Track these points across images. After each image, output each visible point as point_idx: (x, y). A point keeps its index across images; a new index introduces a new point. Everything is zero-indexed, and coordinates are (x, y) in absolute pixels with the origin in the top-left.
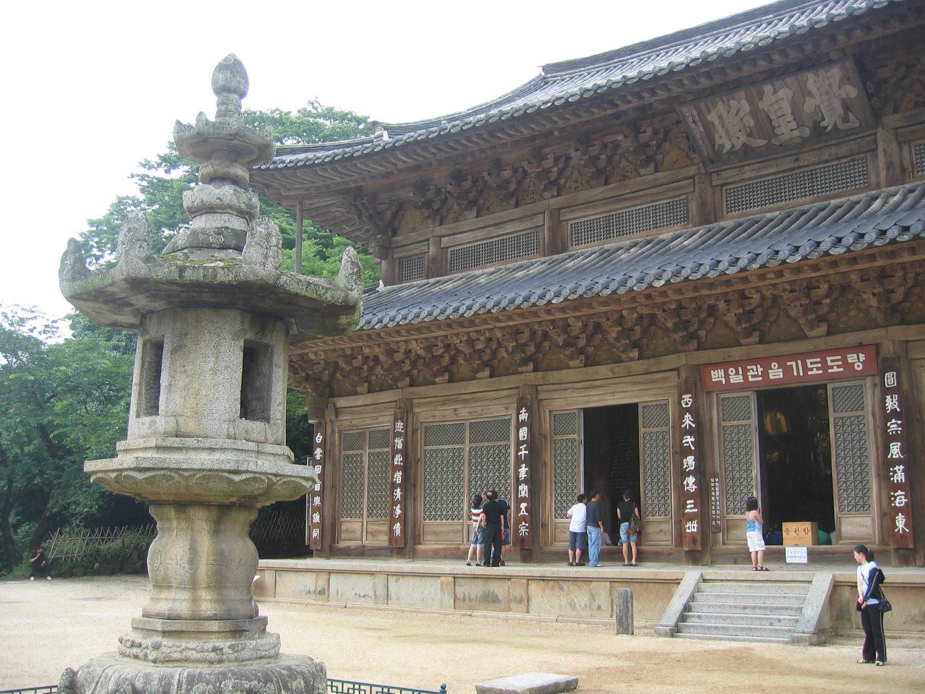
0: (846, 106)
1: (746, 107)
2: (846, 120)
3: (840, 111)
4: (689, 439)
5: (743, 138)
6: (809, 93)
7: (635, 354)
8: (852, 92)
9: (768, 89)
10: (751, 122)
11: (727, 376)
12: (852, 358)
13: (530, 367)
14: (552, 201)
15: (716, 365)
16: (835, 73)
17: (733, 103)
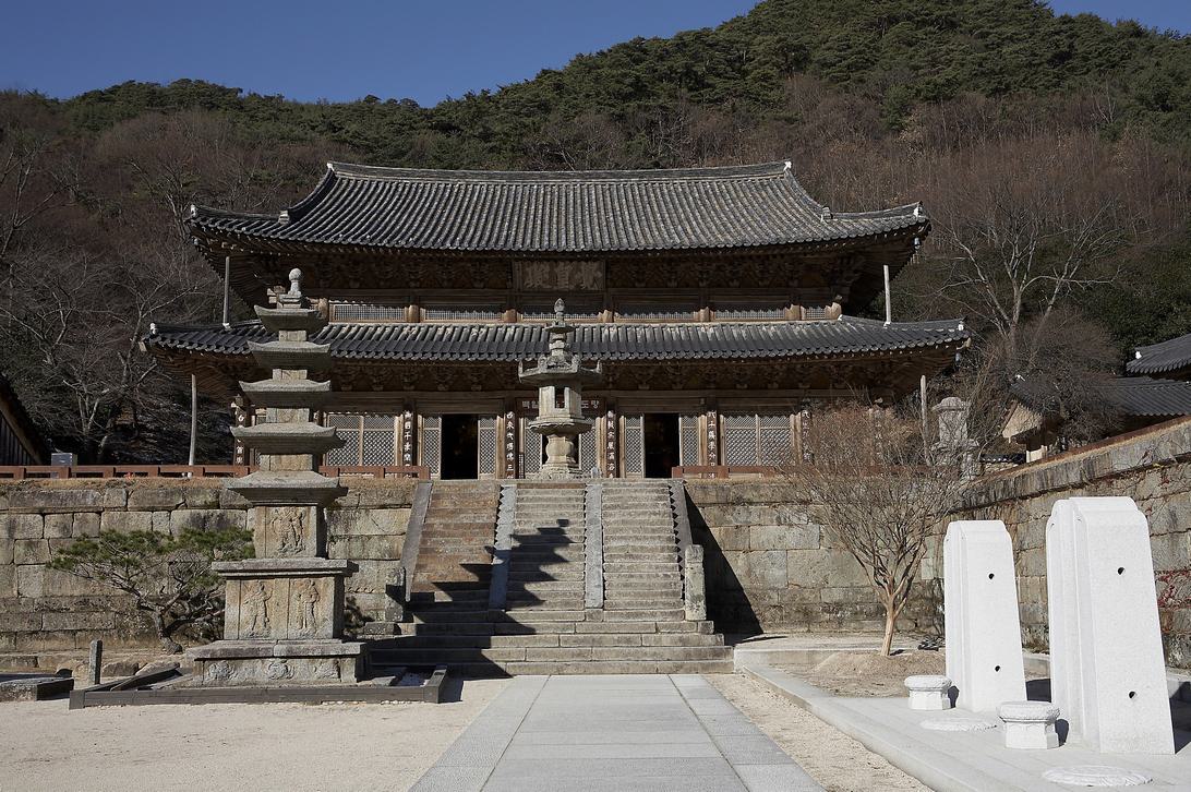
0: (595, 280)
1: (547, 269)
2: (592, 286)
3: (591, 281)
4: (510, 434)
5: (541, 283)
6: (580, 271)
7: (480, 388)
8: (600, 275)
9: (562, 264)
10: (547, 276)
11: (531, 405)
12: (593, 402)
13: (413, 387)
14: (416, 290)
15: (526, 399)
16: (596, 265)
17: (542, 266)
